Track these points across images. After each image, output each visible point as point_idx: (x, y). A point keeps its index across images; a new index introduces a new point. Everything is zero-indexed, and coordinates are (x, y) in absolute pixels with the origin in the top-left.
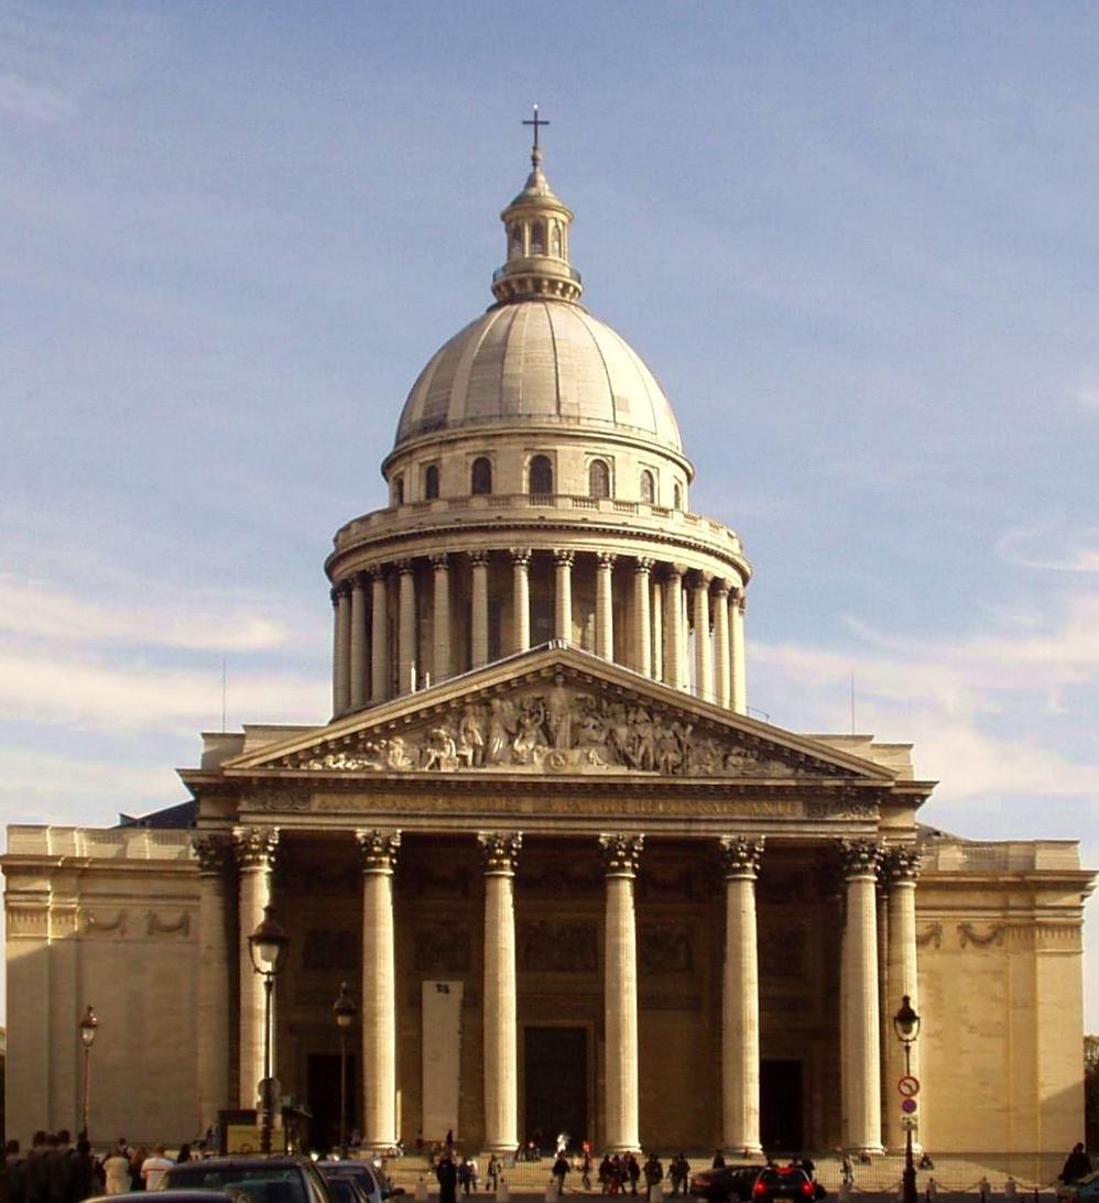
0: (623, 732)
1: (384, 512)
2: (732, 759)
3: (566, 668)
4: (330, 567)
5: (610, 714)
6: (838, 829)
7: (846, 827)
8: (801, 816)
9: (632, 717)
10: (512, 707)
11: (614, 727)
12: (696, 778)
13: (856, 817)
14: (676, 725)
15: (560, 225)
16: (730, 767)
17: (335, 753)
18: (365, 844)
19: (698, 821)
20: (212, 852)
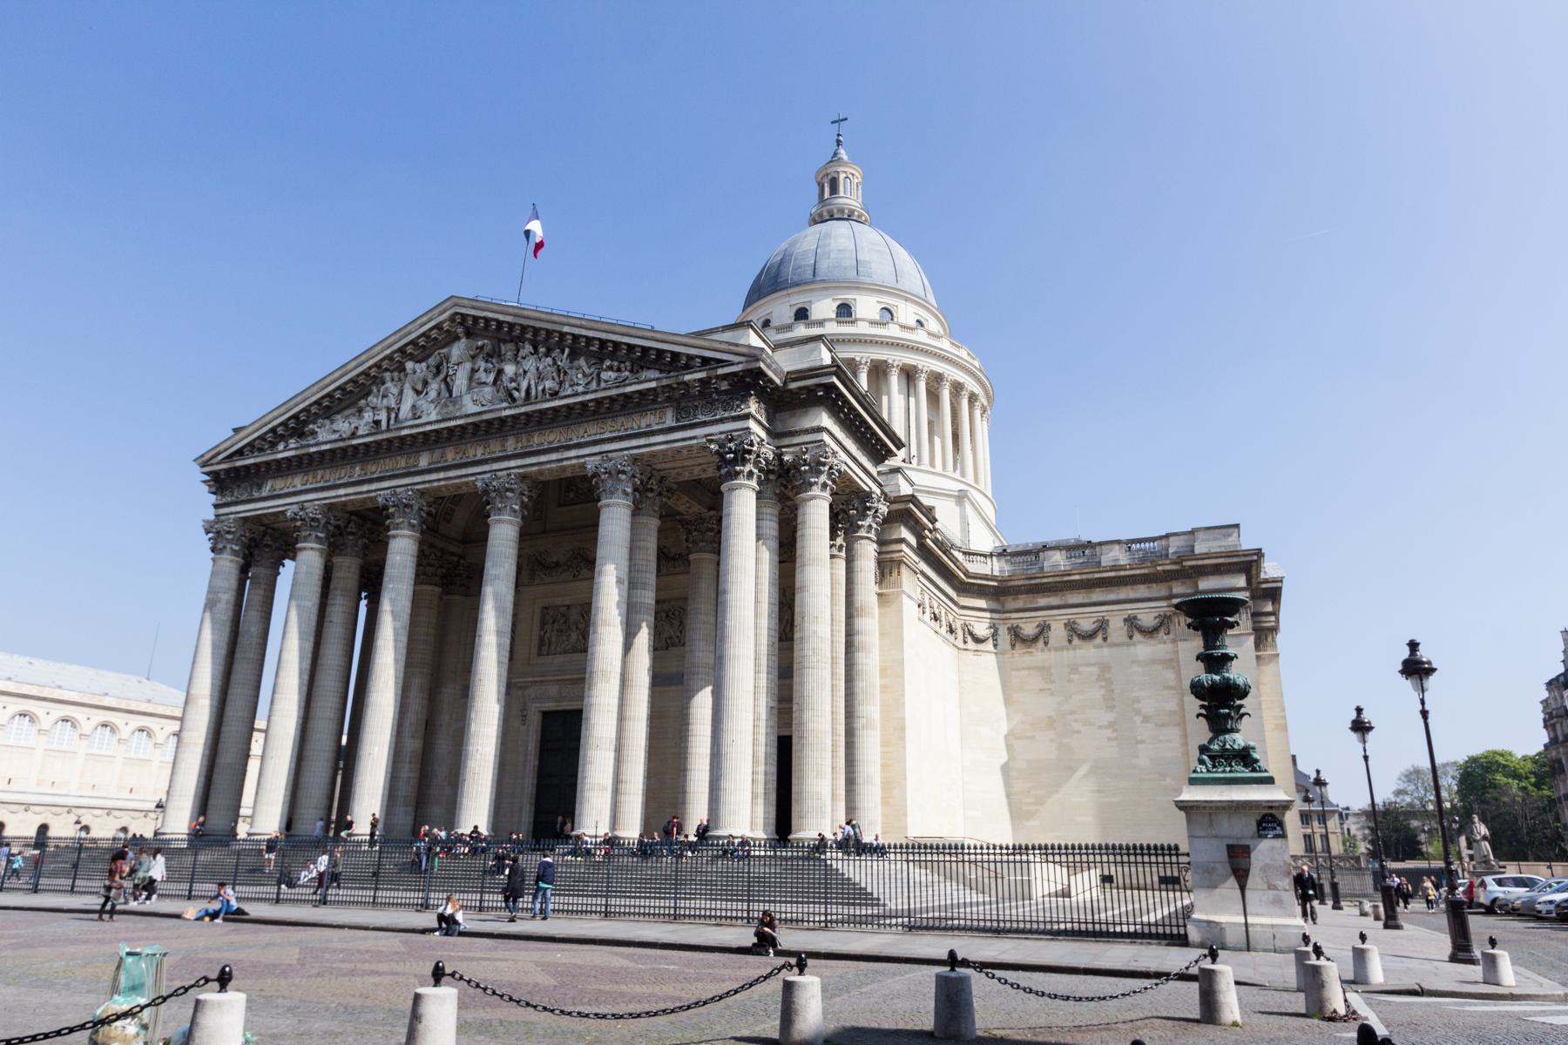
0: (510, 369)
2: (604, 375)
8: (670, 421)
17: (282, 438)
18: (294, 519)
19: (568, 448)
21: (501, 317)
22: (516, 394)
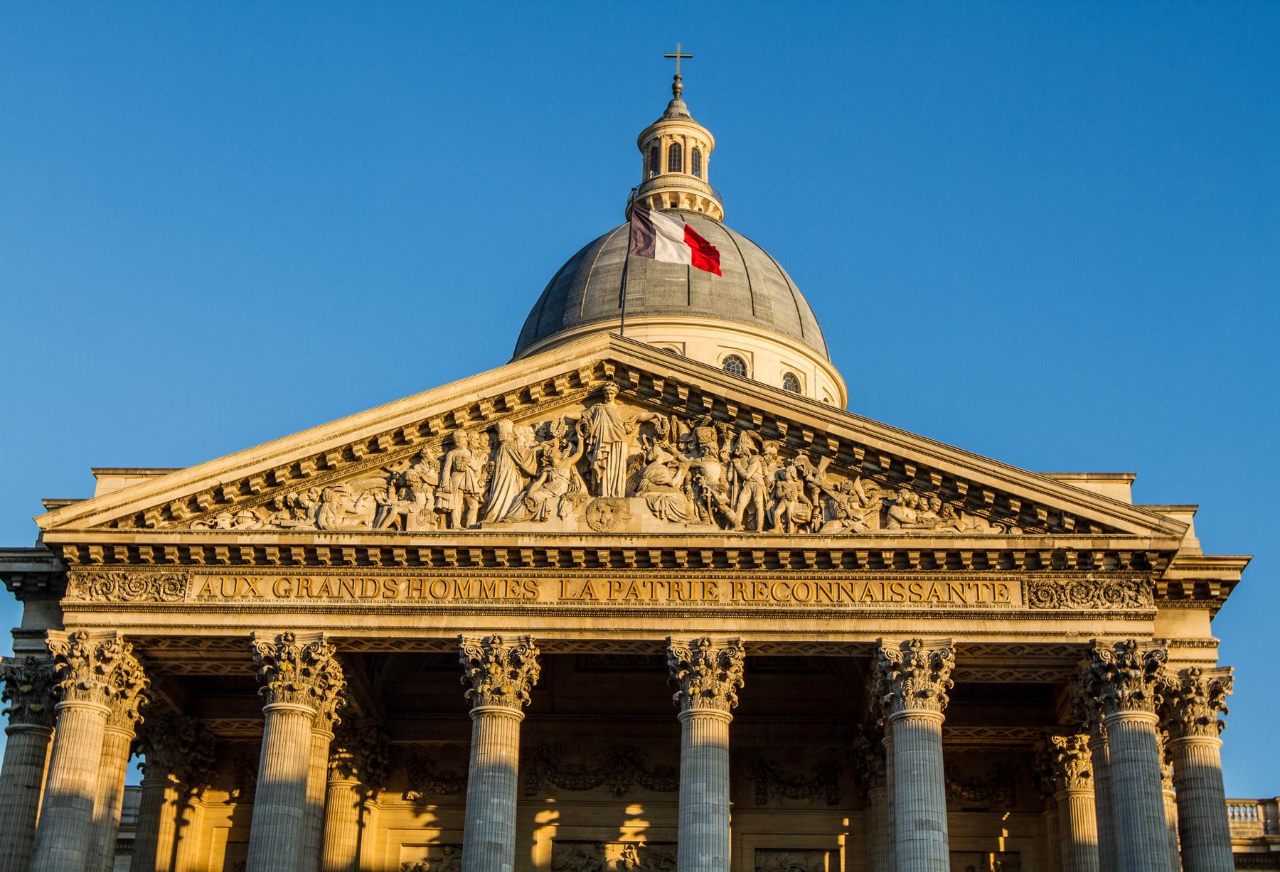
0: (714, 471)
2: (895, 510)
3: (622, 369)
5: (691, 447)
6: (1084, 626)
7: (1103, 625)
8: (1015, 602)
9: (728, 447)
10: (532, 437)
12: (835, 537)
13: (1115, 608)
14: (802, 458)
15: (701, 147)
16: (894, 524)
20: (25, 688)
21: (704, 386)
22: (732, 514)
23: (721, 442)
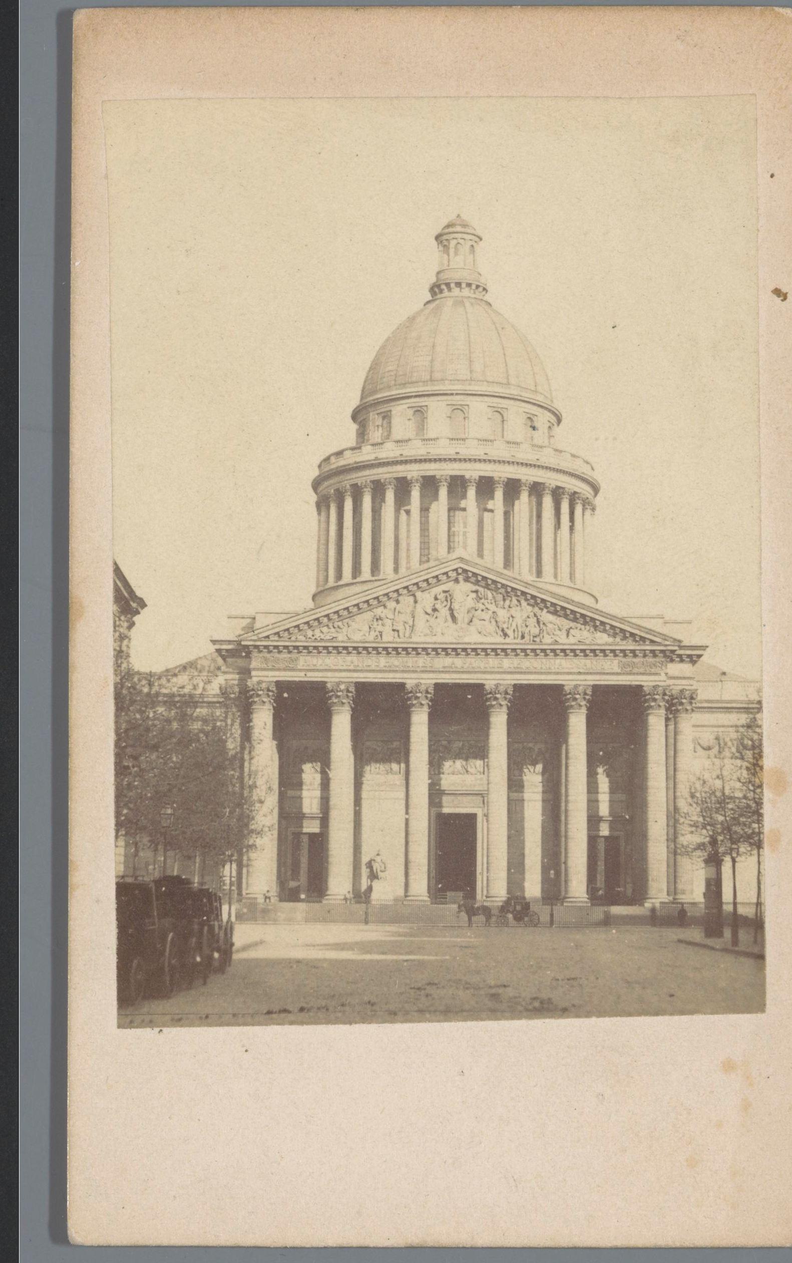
0: (502, 614)
1: (353, 449)
2: (571, 631)
3: (465, 571)
4: (316, 485)
9: (507, 603)
11: (496, 609)
15: (475, 244)
16: (570, 637)
23: (504, 600)
